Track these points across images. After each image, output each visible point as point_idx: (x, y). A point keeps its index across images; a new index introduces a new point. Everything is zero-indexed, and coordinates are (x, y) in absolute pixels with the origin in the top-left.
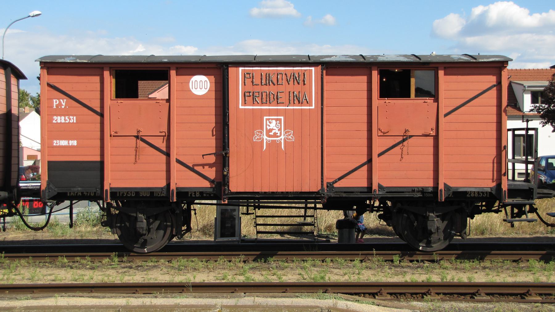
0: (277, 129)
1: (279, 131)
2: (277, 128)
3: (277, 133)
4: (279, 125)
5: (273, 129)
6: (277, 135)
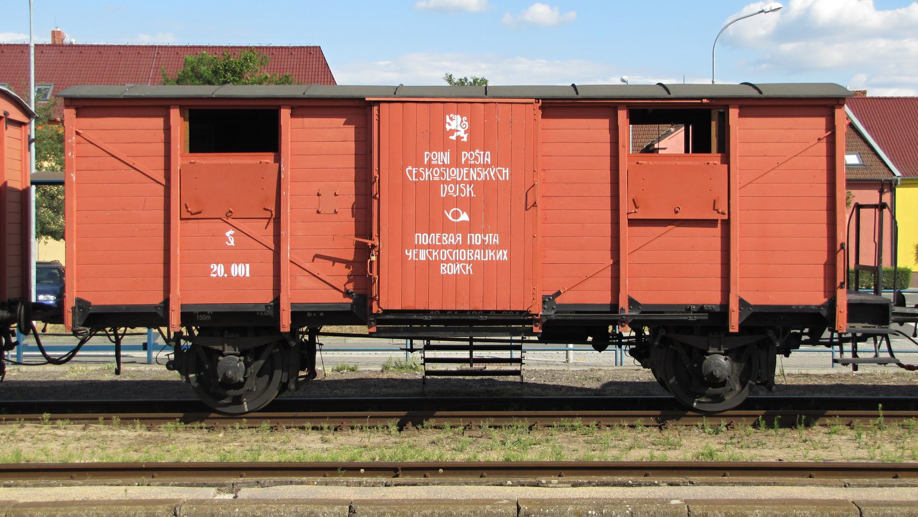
0: (463, 131)
1: (465, 133)
2: (463, 128)
3: (463, 138)
4: (467, 123)
5: (457, 131)
6: (462, 140)
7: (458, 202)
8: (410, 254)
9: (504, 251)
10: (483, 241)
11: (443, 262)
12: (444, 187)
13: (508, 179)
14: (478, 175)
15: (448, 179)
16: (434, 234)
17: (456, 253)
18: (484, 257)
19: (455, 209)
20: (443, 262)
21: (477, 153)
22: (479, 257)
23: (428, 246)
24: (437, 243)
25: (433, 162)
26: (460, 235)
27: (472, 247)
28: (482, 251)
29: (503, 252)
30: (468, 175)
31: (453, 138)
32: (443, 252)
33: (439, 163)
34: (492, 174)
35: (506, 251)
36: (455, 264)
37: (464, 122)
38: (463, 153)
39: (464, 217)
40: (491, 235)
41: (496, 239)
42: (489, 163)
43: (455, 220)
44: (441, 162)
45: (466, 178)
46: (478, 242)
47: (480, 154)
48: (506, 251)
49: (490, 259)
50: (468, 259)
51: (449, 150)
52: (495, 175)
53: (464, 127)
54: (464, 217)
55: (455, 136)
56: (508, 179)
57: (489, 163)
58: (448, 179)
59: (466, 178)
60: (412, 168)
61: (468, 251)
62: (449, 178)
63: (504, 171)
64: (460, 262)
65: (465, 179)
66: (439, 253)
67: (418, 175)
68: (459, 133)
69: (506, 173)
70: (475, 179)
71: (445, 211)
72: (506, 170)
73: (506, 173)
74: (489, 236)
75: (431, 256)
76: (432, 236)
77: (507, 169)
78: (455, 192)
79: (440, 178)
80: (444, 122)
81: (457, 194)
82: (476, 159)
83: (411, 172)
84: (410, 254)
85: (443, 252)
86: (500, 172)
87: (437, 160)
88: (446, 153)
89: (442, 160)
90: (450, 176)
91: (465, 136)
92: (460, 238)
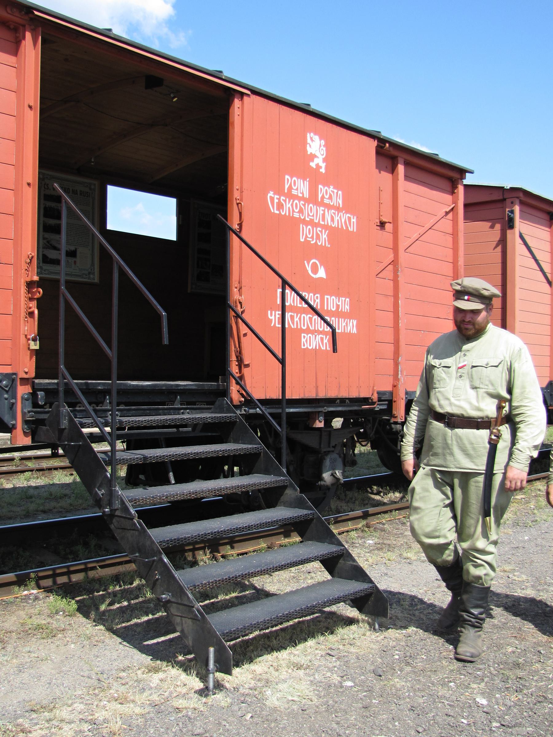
1: (323, 162)
10: (338, 306)
12: (303, 228)
13: (355, 231)
14: (332, 219)
21: (331, 191)
25: (294, 192)
26: (318, 295)
29: (353, 323)
32: (304, 317)
34: (343, 221)
36: (314, 335)
39: (322, 273)
40: (343, 299)
42: (341, 206)
46: (333, 308)
49: (343, 331)
51: (308, 180)
54: (322, 273)
56: (355, 231)
57: (341, 206)
60: (274, 194)
62: (308, 217)
63: (352, 220)
66: (300, 319)
67: (280, 206)
69: (353, 222)
70: (330, 225)
72: (353, 218)
73: (353, 222)
74: (342, 300)
75: (293, 323)
77: (355, 217)
78: (312, 238)
79: (300, 215)
81: (315, 241)
82: (330, 198)
83: (272, 199)
84: (273, 318)
85: (304, 317)
86: (349, 218)
88: (305, 182)
89: (301, 192)
90: (308, 215)
91: (323, 165)
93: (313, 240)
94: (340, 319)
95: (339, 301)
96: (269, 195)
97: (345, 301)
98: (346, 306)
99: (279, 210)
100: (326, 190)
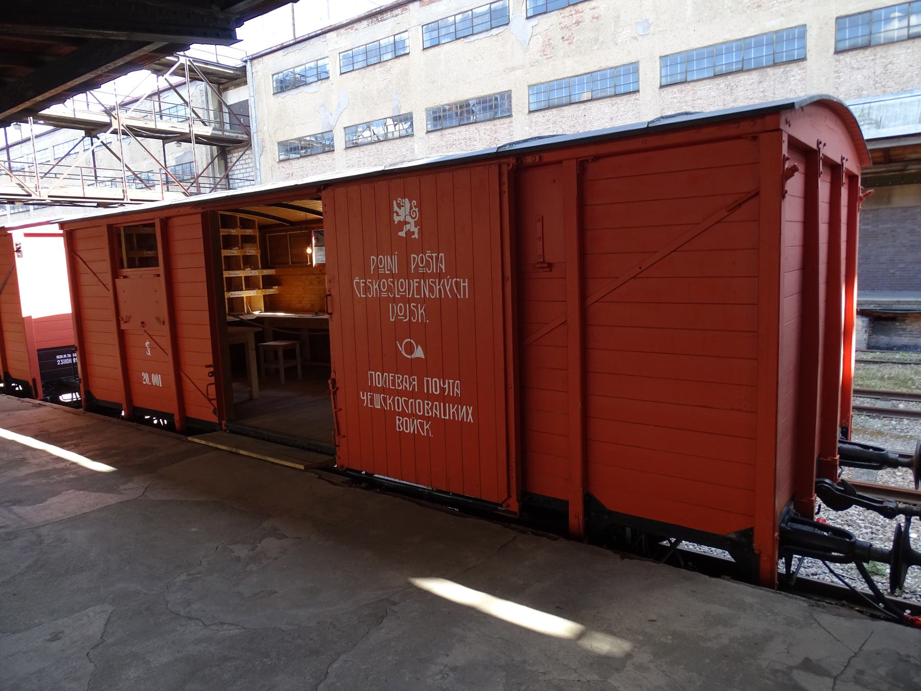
1: (416, 227)
2: (413, 218)
6: (413, 237)
7: (410, 329)
8: (365, 397)
9: (468, 407)
10: (443, 390)
11: (399, 414)
12: (393, 307)
14: (431, 290)
15: (397, 296)
16: (387, 374)
17: (412, 402)
18: (445, 415)
19: (409, 340)
20: (399, 414)
22: (438, 414)
23: (383, 390)
24: (391, 387)
25: (381, 271)
26: (416, 377)
27: (430, 397)
28: (442, 404)
30: (419, 288)
31: (402, 234)
32: (398, 400)
33: (387, 272)
34: (448, 289)
35: (471, 408)
37: (414, 209)
38: (412, 255)
39: (419, 353)
40: (451, 381)
41: (457, 388)
43: (409, 357)
44: (388, 270)
45: (417, 295)
46: (436, 391)
47: (431, 257)
48: (471, 408)
50: (426, 415)
52: (451, 289)
53: (414, 216)
54: (419, 353)
55: (404, 231)
58: (397, 296)
59: (417, 295)
61: (426, 402)
62: (398, 294)
63: (462, 284)
64: (418, 417)
65: (416, 296)
66: (393, 401)
67: (367, 289)
68: (408, 227)
69: (464, 287)
71: (397, 342)
72: (464, 282)
73: (464, 287)
74: (449, 383)
76: (386, 375)
78: (405, 316)
80: (391, 211)
81: (408, 318)
82: (428, 265)
83: (358, 284)
84: (365, 398)
85: (398, 400)
86: (457, 284)
87: (384, 267)
88: (393, 256)
92: (416, 383)
93: (405, 318)
94: (447, 404)
95: (444, 384)
96: (355, 281)
97: (453, 384)
98: (456, 389)
99: (366, 294)
100: (422, 257)
